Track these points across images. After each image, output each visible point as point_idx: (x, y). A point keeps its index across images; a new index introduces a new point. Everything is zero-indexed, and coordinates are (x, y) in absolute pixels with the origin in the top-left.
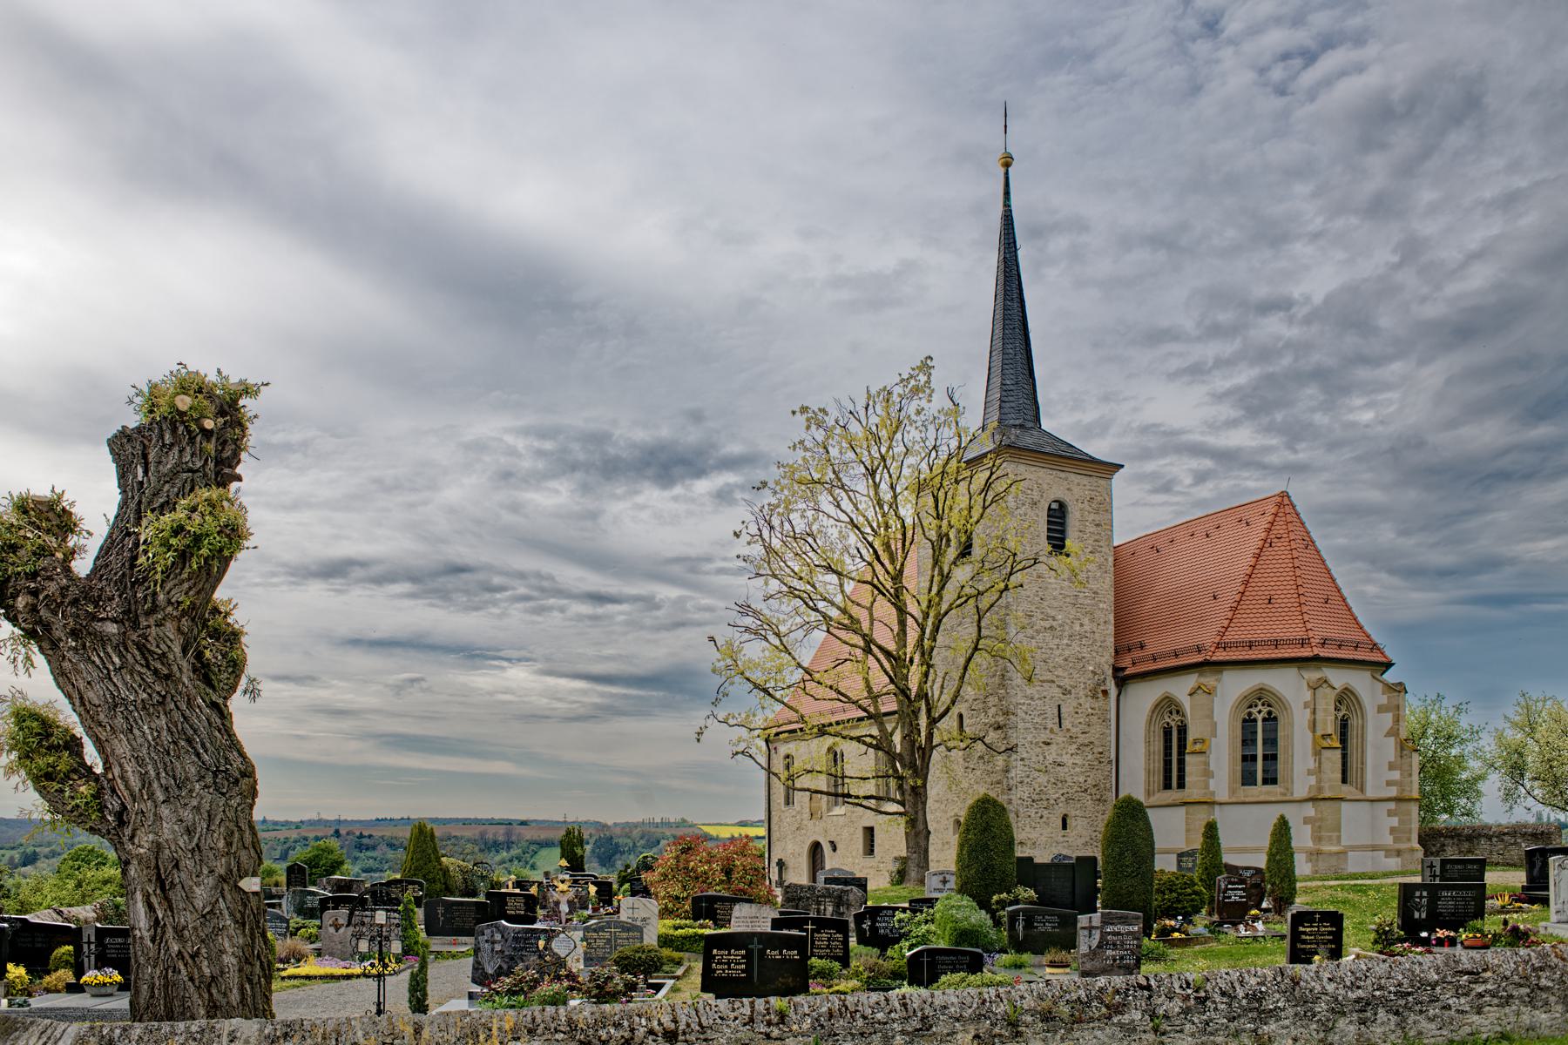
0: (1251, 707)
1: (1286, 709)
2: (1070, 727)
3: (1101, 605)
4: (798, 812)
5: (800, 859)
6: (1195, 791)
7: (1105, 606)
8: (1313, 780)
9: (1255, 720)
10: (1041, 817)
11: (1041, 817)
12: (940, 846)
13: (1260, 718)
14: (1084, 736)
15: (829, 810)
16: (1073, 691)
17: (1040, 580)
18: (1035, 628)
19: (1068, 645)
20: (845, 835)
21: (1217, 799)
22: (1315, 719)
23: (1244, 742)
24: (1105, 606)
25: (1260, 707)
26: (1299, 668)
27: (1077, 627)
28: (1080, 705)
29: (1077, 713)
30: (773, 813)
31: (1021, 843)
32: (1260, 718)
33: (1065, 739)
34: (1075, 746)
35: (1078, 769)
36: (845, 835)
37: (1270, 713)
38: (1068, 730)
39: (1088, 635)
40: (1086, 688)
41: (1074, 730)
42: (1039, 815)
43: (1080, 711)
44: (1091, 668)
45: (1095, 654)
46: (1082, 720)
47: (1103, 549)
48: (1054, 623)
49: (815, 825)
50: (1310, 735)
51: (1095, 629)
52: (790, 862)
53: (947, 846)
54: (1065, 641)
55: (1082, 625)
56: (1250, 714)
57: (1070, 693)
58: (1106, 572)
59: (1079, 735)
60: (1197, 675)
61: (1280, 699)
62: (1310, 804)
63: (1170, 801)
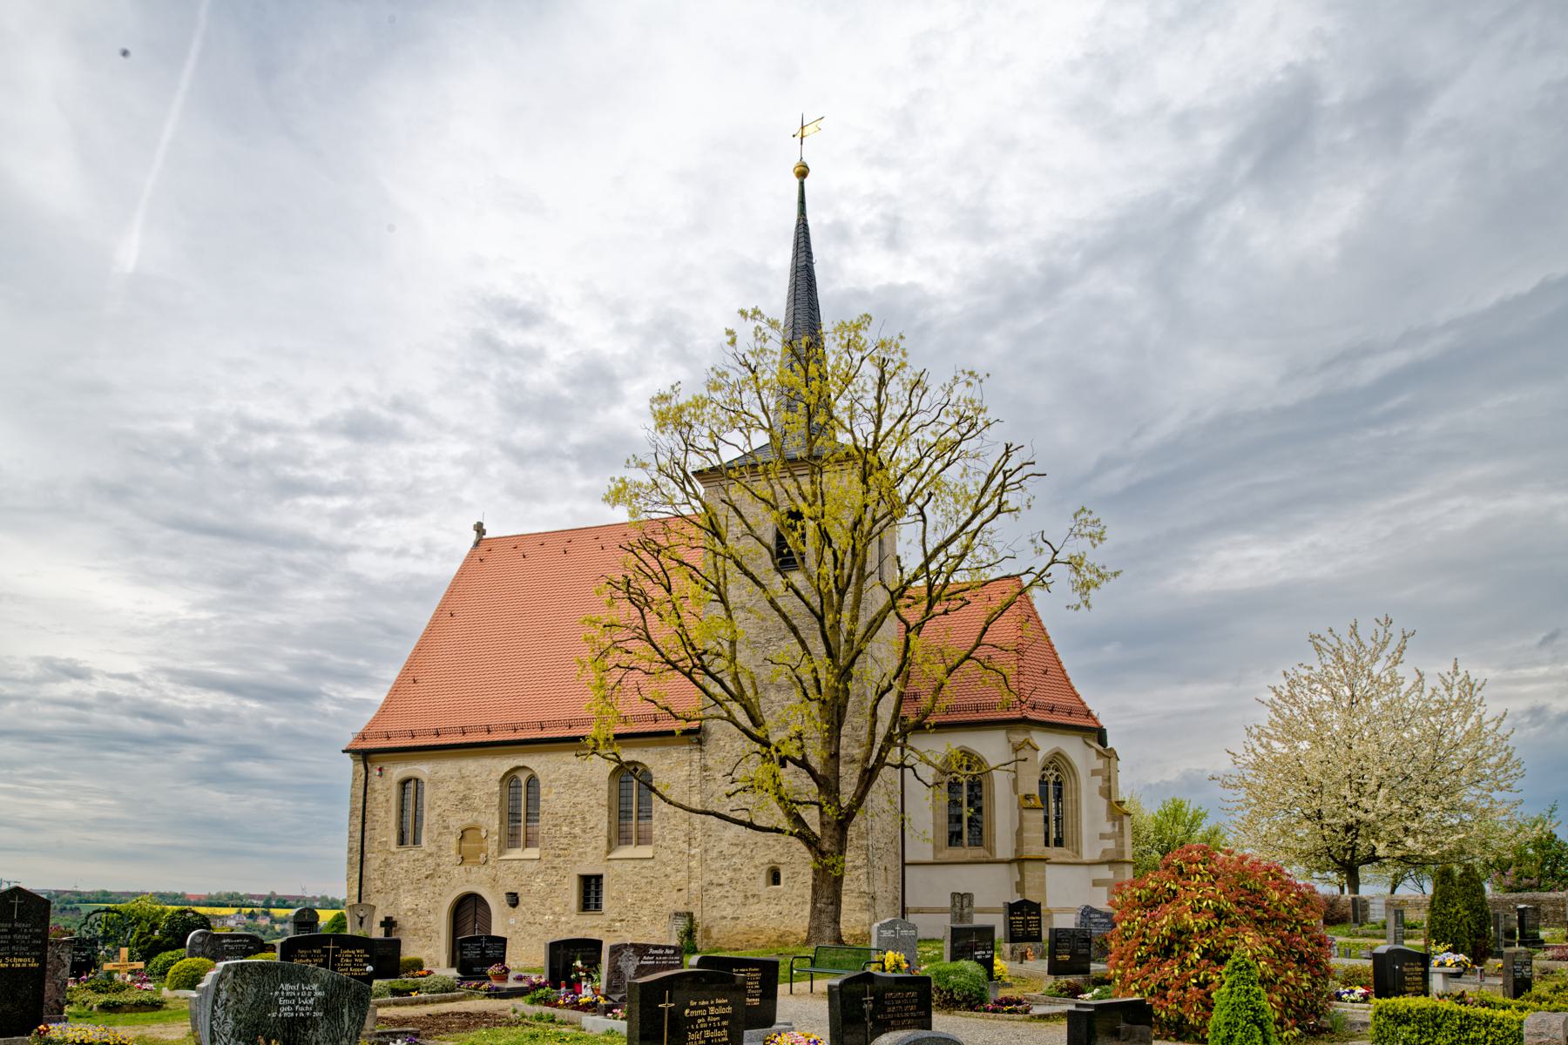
0: (1044, 769)
1: (1074, 775)
4: (430, 855)
5: (431, 918)
6: (1034, 847)
8: (1110, 844)
12: (740, 899)
15: (501, 853)
20: (538, 884)
22: (1110, 787)
26: (1084, 737)
30: (368, 855)
32: (1052, 779)
36: (538, 884)
37: (1057, 777)
49: (468, 872)
50: (1106, 801)
52: (406, 922)
53: (751, 900)
60: (1004, 731)
61: (1069, 764)
62: (1106, 867)
63: (968, 857)
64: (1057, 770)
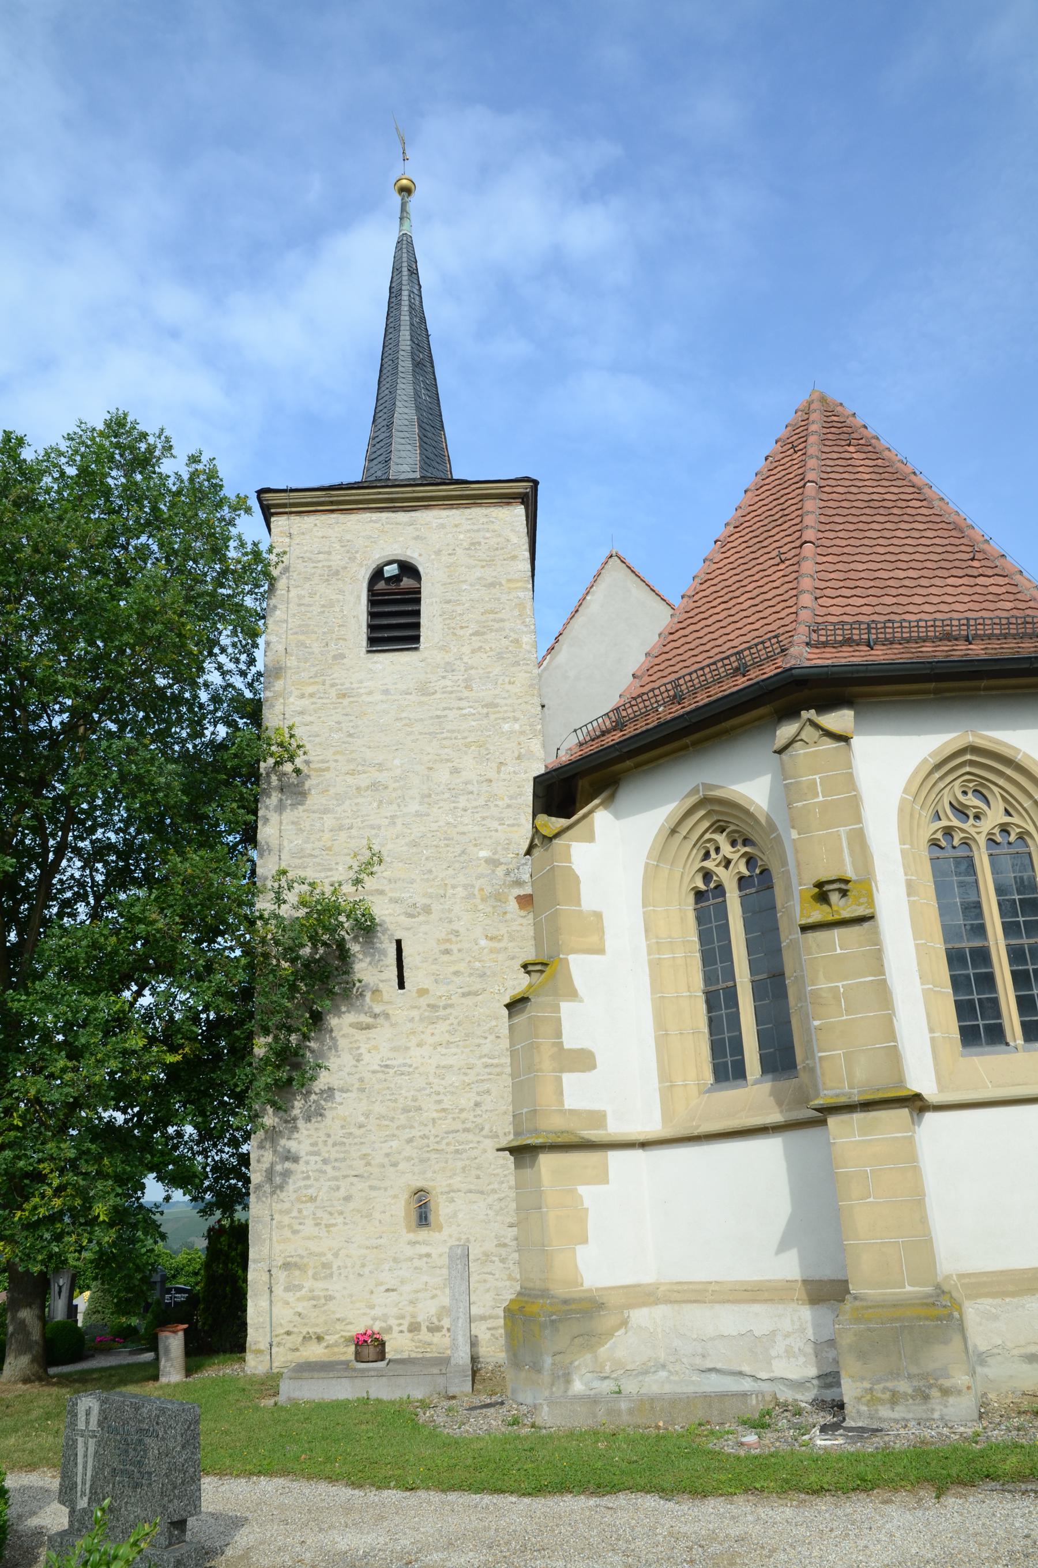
2: (427, 983)
3: (506, 727)
7: (517, 727)
9: (720, 889)
10: (348, 1199)
11: (348, 1199)
13: (728, 878)
14: (469, 1001)
16: (435, 907)
17: (346, 702)
18: (332, 791)
19: (418, 814)
21: (616, 1128)
23: (707, 959)
24: (517, 727)
25: (726, 849)
27: (443, 775)
28: (457, 933)
29: (447, 952)
31: (286, 1266)
33: (415, 1013)
34: (443, 1027)
35: (452, 1079)
38: (422, 992)
39: (470, 787)
40: (471, 896)
41: (442, 990)
42: (342, 1193)
43: (454, 948)
44: (484, 854)
45: (495, 825)
46: (462, 967)
47: (507, 625)
48: (383, 777)
51: (492, 774)
54: (414, 807)
55: (455, 771)
56: (707, 875)
57: (427, 910)
58: (517, 663)
59: (455, 999)
64: (746, 842)
